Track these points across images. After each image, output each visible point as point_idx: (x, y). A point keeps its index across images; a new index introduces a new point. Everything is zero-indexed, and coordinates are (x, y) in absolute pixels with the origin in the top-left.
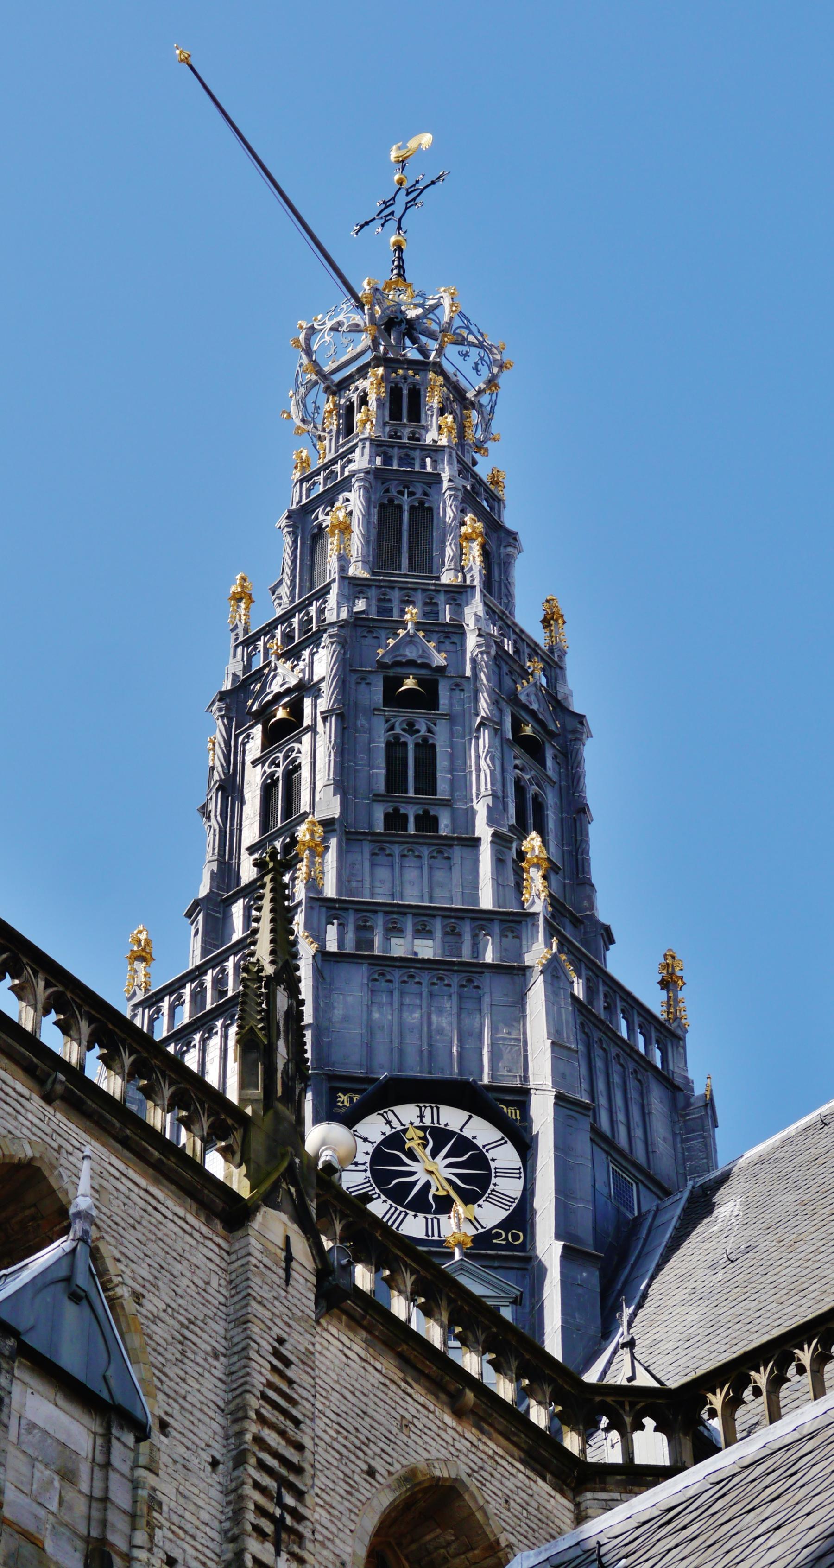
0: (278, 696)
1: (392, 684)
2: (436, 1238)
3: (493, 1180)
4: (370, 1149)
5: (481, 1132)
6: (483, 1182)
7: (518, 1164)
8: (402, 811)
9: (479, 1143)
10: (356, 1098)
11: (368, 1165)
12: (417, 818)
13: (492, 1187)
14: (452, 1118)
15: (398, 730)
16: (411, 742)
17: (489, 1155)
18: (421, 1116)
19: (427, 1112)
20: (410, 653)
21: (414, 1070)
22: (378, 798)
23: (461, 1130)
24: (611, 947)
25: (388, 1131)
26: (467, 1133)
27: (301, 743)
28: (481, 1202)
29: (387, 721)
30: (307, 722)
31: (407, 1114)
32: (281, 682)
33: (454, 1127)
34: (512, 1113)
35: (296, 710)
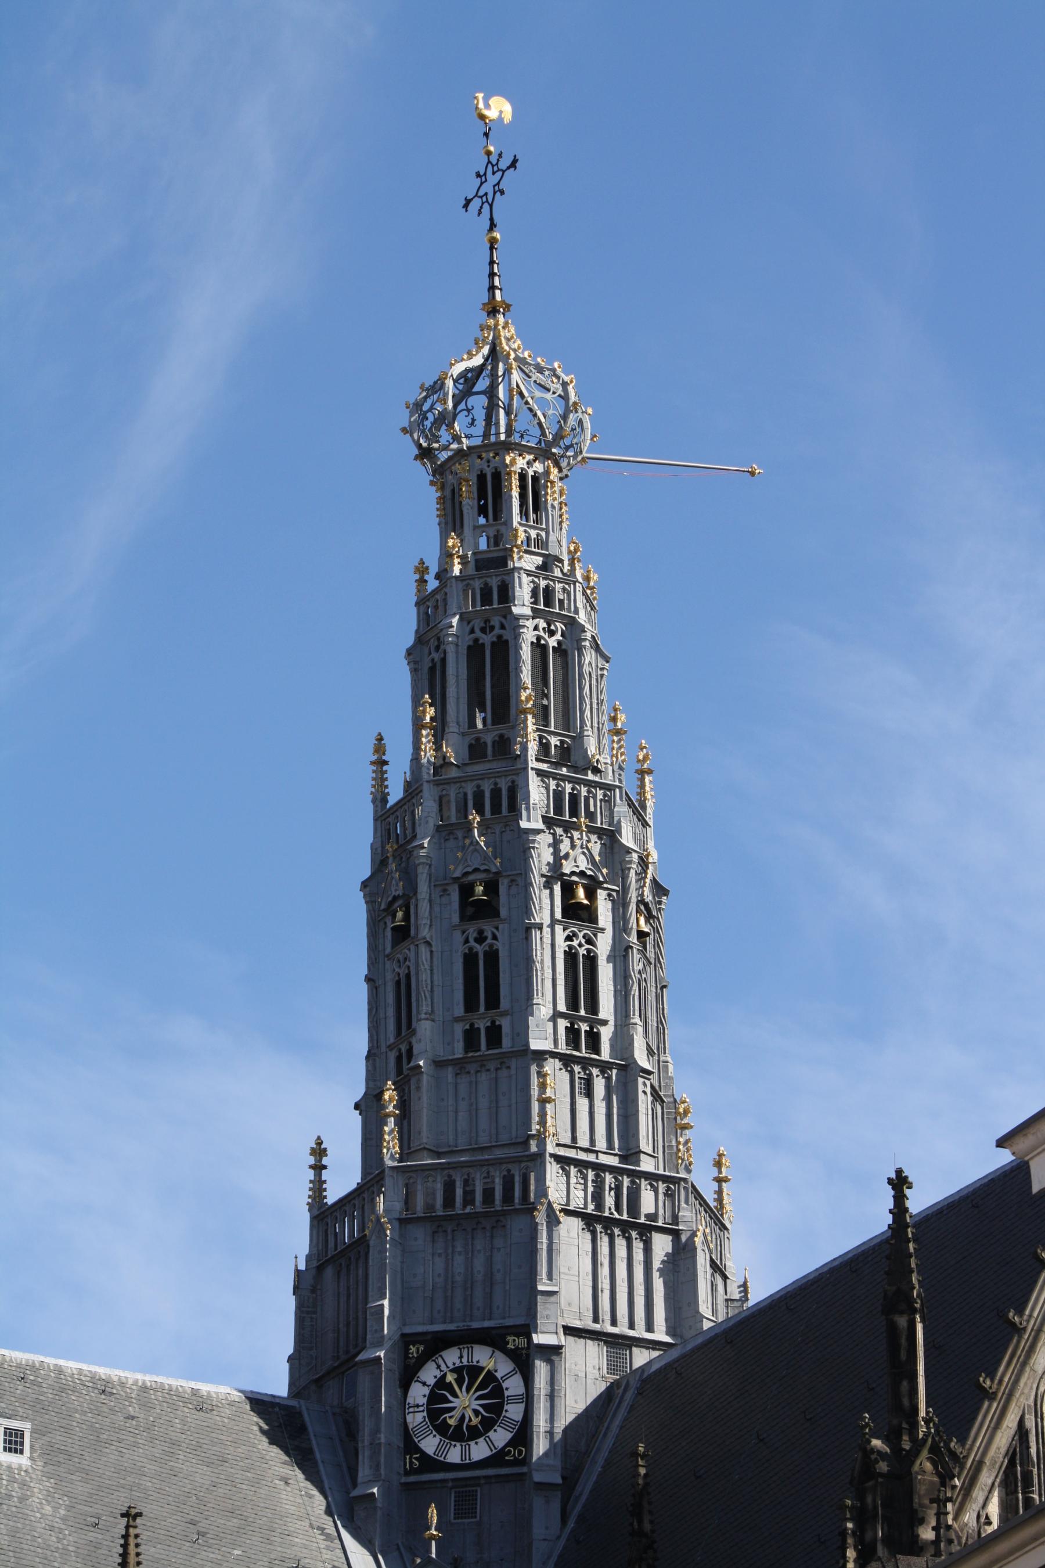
3: (506, 1407)
4: (426, 1391)
10: (422, 1348)
22: (457, 1020)
31: (452, 1357)
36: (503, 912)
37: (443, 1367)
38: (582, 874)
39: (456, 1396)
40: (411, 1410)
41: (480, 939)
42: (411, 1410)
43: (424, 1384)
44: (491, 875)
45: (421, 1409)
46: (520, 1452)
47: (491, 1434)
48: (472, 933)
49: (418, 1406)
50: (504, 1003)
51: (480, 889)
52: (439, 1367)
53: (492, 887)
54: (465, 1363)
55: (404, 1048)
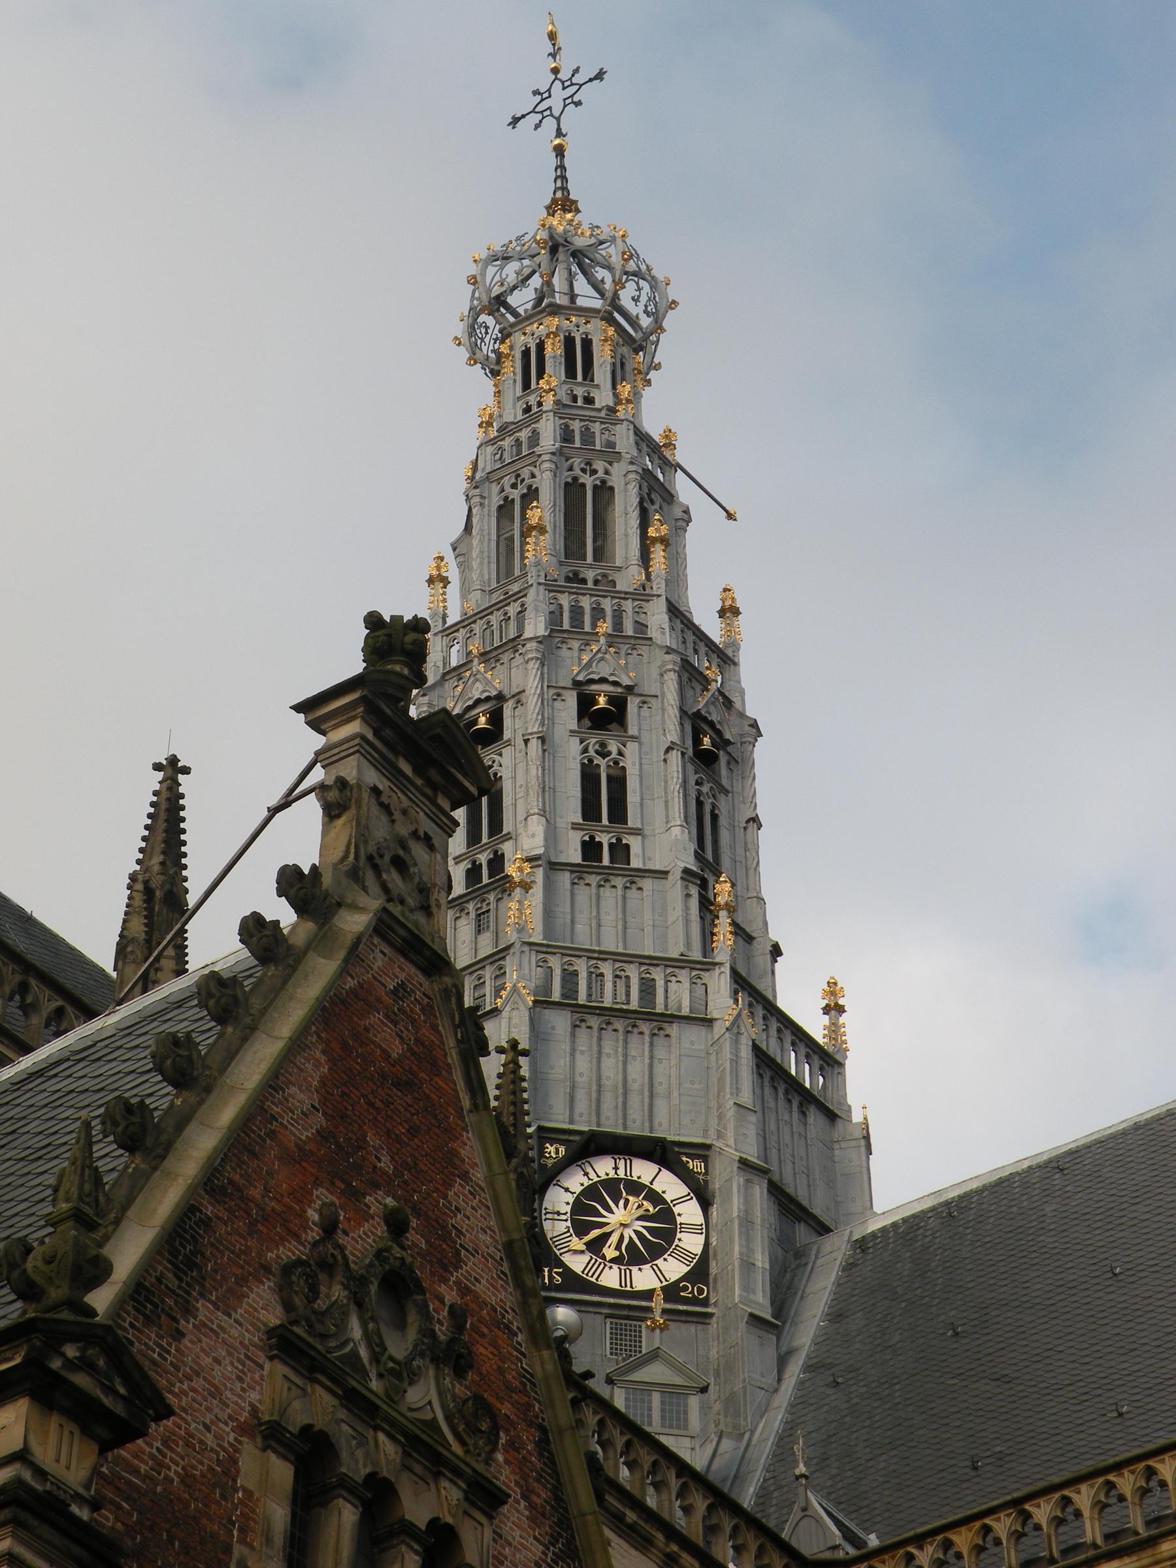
0: (478, 702)
1: (585, 702)
2: (628, 1288)
3: (679, 1235)
5: (670, 1186)
7: (700, 1219)
9: (668, 1197)
12: (611, 845)
14: (643, 1171)
15: (592, 753)
17: (676, 1210)
18: (616, 1168)
19: (621, 1164)
20: (604, 670)
21: (611, 1124)
22: (575, 827)
23: (651, 1183)
26: (657, 1187)
27: (501, 755)
28: (666, 1256)
30: (507, 734)
31: (604, 1167)
32: (481, 689)
33: (646, 1180)
34: (696, 1166)
35: (496, 718)
36: (632, 730)
37: (592, 1175)
38: (711, 724)
39: (612, 1212)
40: (549, 1216)
41: (604, 754)
42: (549, 1216)
43: (567, 1190)
44: (620, 690)
45: (564, 1217)
46: (701, 1291)
47: (660, 1262)
49: (558, 1213)
50: (633, 821)
51: (602, 701)
52: (586, 1174)
53: (619, 704)
54: (622, 1175)
55: (483, 858)
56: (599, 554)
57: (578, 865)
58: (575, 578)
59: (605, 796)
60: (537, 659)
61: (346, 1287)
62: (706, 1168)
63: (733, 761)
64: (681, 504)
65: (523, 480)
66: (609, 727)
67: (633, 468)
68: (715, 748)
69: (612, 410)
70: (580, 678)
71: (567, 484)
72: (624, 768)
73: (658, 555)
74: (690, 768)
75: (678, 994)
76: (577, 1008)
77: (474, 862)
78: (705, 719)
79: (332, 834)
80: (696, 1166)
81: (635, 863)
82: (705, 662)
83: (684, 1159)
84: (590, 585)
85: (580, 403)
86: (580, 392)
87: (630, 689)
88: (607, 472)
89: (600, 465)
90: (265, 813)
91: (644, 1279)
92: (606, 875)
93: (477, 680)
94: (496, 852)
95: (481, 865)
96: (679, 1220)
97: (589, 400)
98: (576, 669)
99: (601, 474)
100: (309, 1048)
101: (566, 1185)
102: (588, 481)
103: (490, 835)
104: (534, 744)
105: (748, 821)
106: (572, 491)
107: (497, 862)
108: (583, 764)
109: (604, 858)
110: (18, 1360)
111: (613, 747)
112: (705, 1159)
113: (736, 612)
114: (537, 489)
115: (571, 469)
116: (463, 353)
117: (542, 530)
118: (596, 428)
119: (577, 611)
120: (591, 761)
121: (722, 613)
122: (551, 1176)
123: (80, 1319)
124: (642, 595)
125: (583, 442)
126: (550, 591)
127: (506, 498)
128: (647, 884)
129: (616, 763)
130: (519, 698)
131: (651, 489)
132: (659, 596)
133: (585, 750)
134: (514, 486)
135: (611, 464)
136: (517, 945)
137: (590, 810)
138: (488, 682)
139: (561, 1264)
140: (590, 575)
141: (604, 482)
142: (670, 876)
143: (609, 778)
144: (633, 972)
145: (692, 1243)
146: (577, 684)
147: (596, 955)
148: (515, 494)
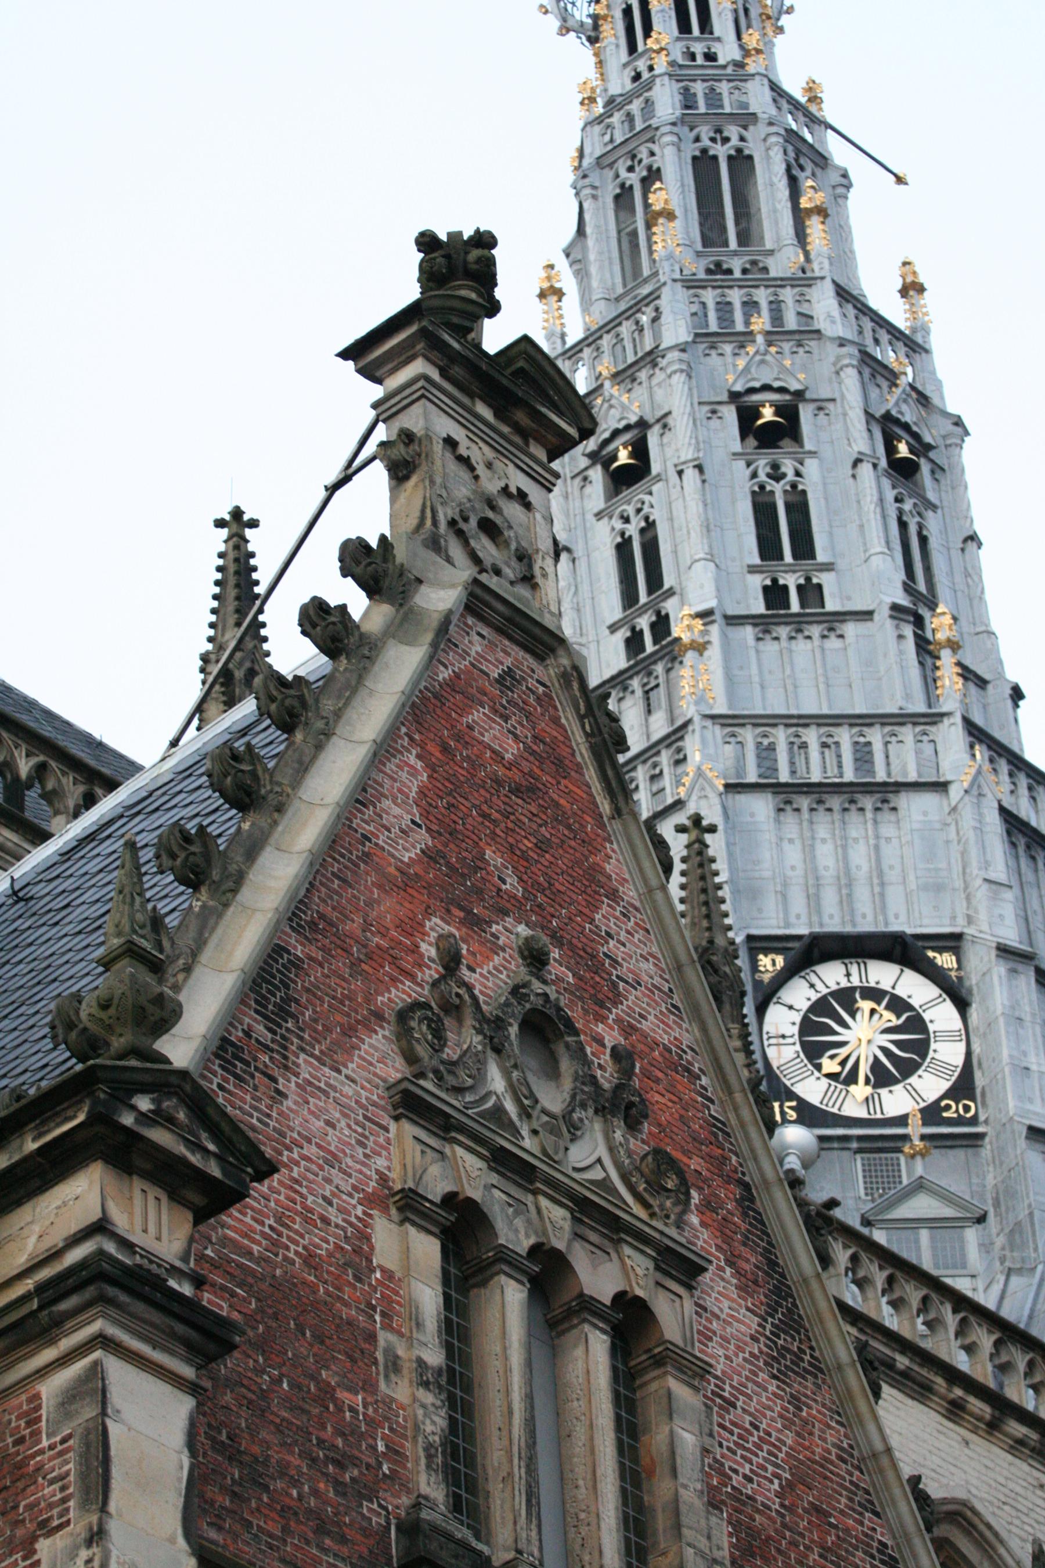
0: (616, 433)
1: (747, 417)
2: (879, 1116)
3: (933, 1046)
4: (797, 1018)
5: (915, 988)
6: (922, 1048)
7: (957, 1023)
8: (781, 582)
9: (915, 1002)
11: (797, 1037)
13: (931, 1054)
14: (882, 974)
15: (762, 477)
16: (778, 489)
17: (927, 1016)
18: (848, 975)
20: (766, 376)
21: (833, 923)
23: (893, 988)
24: (1021, 703)
25: (814, 996)
26: (901, 992)
27: (650, 493)
29: (748, 465)
30: (655, 468)
31: (832, 975)
32: (618, 417)
33: (885, 985)
34: (946, 960)
35: (640, 450)
37: (819, 986)
38: (906, 427)
40: (773, 1041)
41: (777, 475)
43: (791, 1007)
46: (967, 1109)
47: (913, 1080)
48: (762, 465)
49: (783, 1037)
50: (821, 556)
51: (768, 414)
53: (789, 413)
55: (644, 623)
56: (744, 238)
57: (761, 616)
58: (718, 268)
59: (783, 527)
60: (682, 371)
61: (479, 1031)
62: (958, 961)
63: (937, 469)
64: (837, 168)
65: (640, 161)
66: (781, 443)
67: (774, 129)
68: (912, 453)
69: (740, 65)
70: (738, 388)
71: (695, 158)
72: (804, 492)
73: (815, 227)
74: (886, 483)
75: (901, 757)
76: (778, 788)
77: (633, 629)
78: (897, 422)
79: (403, 497)
80: (946, 960)
81: (832, 604)
82: (889, 351)
83: (931, 954)
84: (737, 274)
85: (700, 60)
86: (699, 48)
87: (799, 395)
88: (742, 139)
89: (732, 131)
90: (323, 494)
91: (896, 1101)
92: (798, 623)
93: (611, 406)
94: (658, 613)
95: (641, 631)
96: (931, 1028)
97: (710, 57)
98: (731, 378)
99: (735, 141)
100: (401, 753)
101: (789, 1002)
102: (721, 152)
103: (650, 591)
104: (690, 474)
105: (965, 540)
106: (703, 165)
107: (661, 625)
108: (753, 493)
109: (791, 606)
110: (81, 1118)
111: (788, 467)
112: (956, 951)
113: (921, 289)
114: (659, 170)
115: (697, 139)
116: (553, 22)
117: (670, 216)
118: (724, 87)
119: (724, 308)
120: (762, 487)
121: (904, 292)
122: (767, 995)
123: (148, 1065)
124: (803, 280)
125: (709, 106)
126: (688, 288)
127: (622, 186)
128: (850, 629)
129: (794, 486)
130: (664, 421)
131: (798, 153)
132: (822, 278)
133: (754, 475)
134: (631, 169)
135: (745, 128)
136: (697, 719)
137: (769, 548)
138: (624, 408)
139: (791, 1095)
140: (736, 265)
141: (739, 151)
142: (876, 616)
143: (788, 506)
144: (845, 737)
145: (949, 1053)
146: (734, 396)
147: (795, 721)
148: (633, 179)
